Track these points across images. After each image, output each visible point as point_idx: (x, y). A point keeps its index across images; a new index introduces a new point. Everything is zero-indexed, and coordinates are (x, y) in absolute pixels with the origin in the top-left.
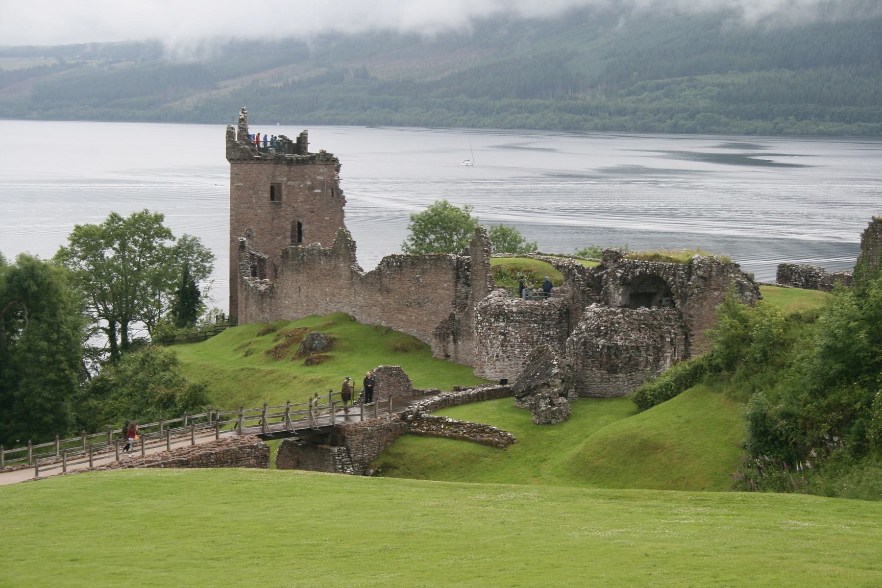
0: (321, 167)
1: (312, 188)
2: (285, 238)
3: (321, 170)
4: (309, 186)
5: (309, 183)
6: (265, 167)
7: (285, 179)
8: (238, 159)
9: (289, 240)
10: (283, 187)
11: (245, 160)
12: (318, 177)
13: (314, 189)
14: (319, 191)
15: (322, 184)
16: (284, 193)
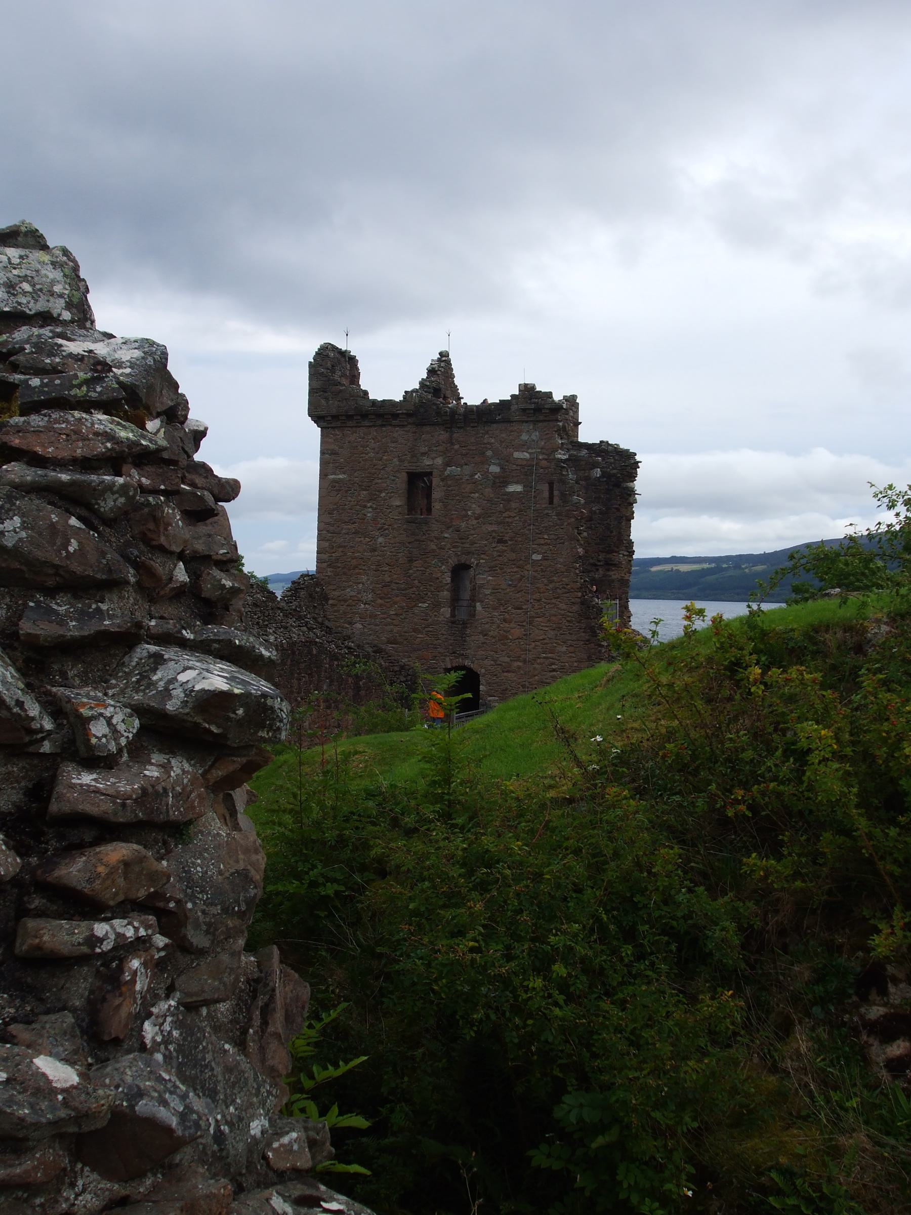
0: (525, 427)
1: (502, 481)
2: (436, 606)
3: (525, 437)
4: (496, 476)
5: (495, 469)
6: (398, 433)
7: (439, 461)
8: (335, 417)
9: (446, 611)
10: (435, 481)
11: (350, 417)
12: (517, 455)
13: (506, 483)
14: (518, 488)
15: (525, 472)
16: (437, 494)
